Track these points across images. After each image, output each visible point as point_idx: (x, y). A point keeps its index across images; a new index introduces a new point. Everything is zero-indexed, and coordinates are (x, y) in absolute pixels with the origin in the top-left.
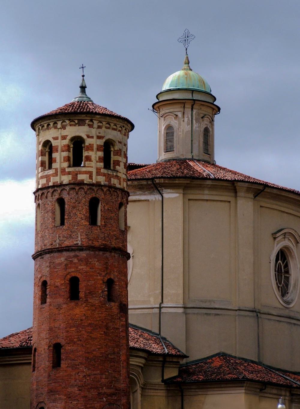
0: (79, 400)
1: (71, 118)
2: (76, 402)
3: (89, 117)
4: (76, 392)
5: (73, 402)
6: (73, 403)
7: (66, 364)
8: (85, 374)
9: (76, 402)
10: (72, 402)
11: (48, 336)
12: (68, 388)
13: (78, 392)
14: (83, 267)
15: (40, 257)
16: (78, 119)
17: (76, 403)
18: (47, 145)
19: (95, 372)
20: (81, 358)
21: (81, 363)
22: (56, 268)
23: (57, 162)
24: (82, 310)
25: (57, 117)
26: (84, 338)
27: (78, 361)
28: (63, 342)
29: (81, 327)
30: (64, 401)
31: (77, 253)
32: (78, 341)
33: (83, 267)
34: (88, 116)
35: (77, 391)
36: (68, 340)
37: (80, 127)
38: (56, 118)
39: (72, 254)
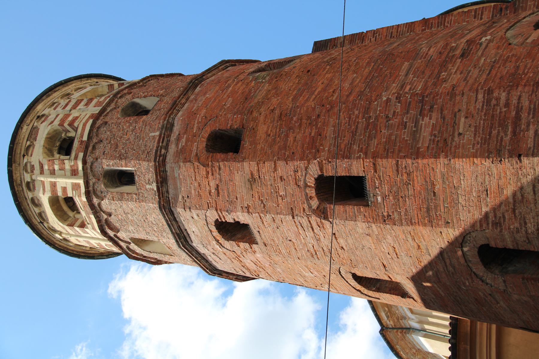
0: (457, 110)
1: (22, 153)
2: (460, 120)
3: (31, 121)
4: (433, 121)
5: (458, 128)
6: (461, 131)
7: (360, 155)
8: (393, 99)
9: (463, 119)
10: (460, 134)
11: (305, 221)
12: (419, 148)
13: (434, 115)
14: (196, 122)
15: (190, 243)
16: (27, 141)
17: (466, 117)
18: (68, 215)
19: (403, 73)
20: (354, 113)
21: (367, 110)
22: (190, 193)
23: (65, 186)
24: (262, 118)
25: (19, 182)
26: (314, 109)
27: (358, 122)
28: (314, 171)
29: (292, 118)
30: (452, 160)
31: (173, 137)
32: (316, 125)
33: (196, 122)
34: (28, 122)
35: (430, 119)
36: (310, 153)
37: (38, 139)
38: (21, 182)
39: (172, 148)
